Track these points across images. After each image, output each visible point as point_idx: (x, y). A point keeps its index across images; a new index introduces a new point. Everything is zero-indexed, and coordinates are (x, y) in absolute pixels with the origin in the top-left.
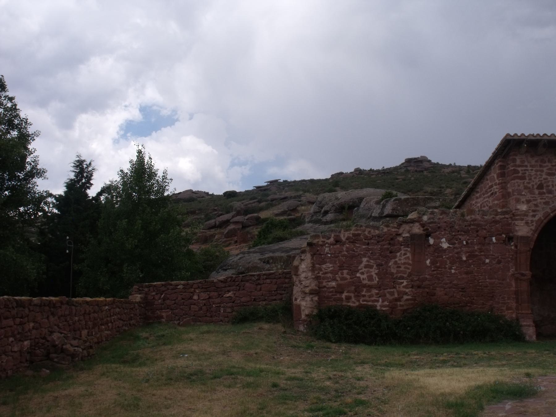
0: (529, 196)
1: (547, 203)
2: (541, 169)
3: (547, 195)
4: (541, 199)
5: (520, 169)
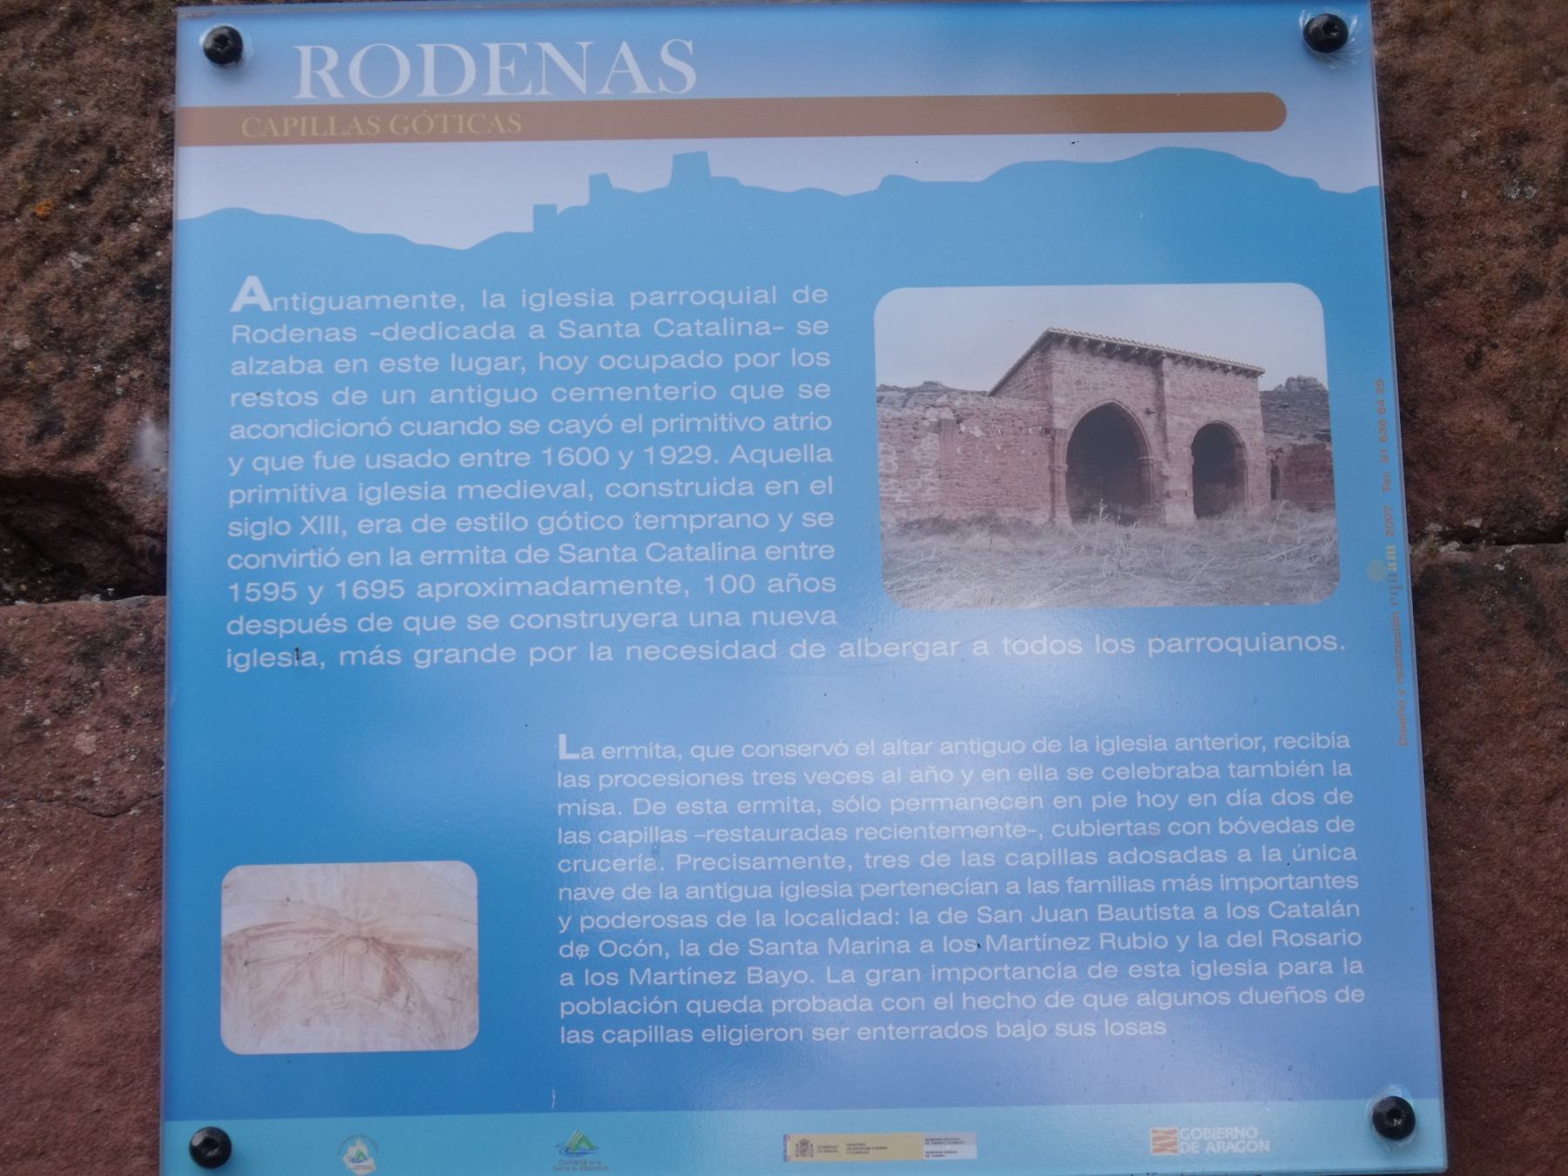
1: (1084, 399)
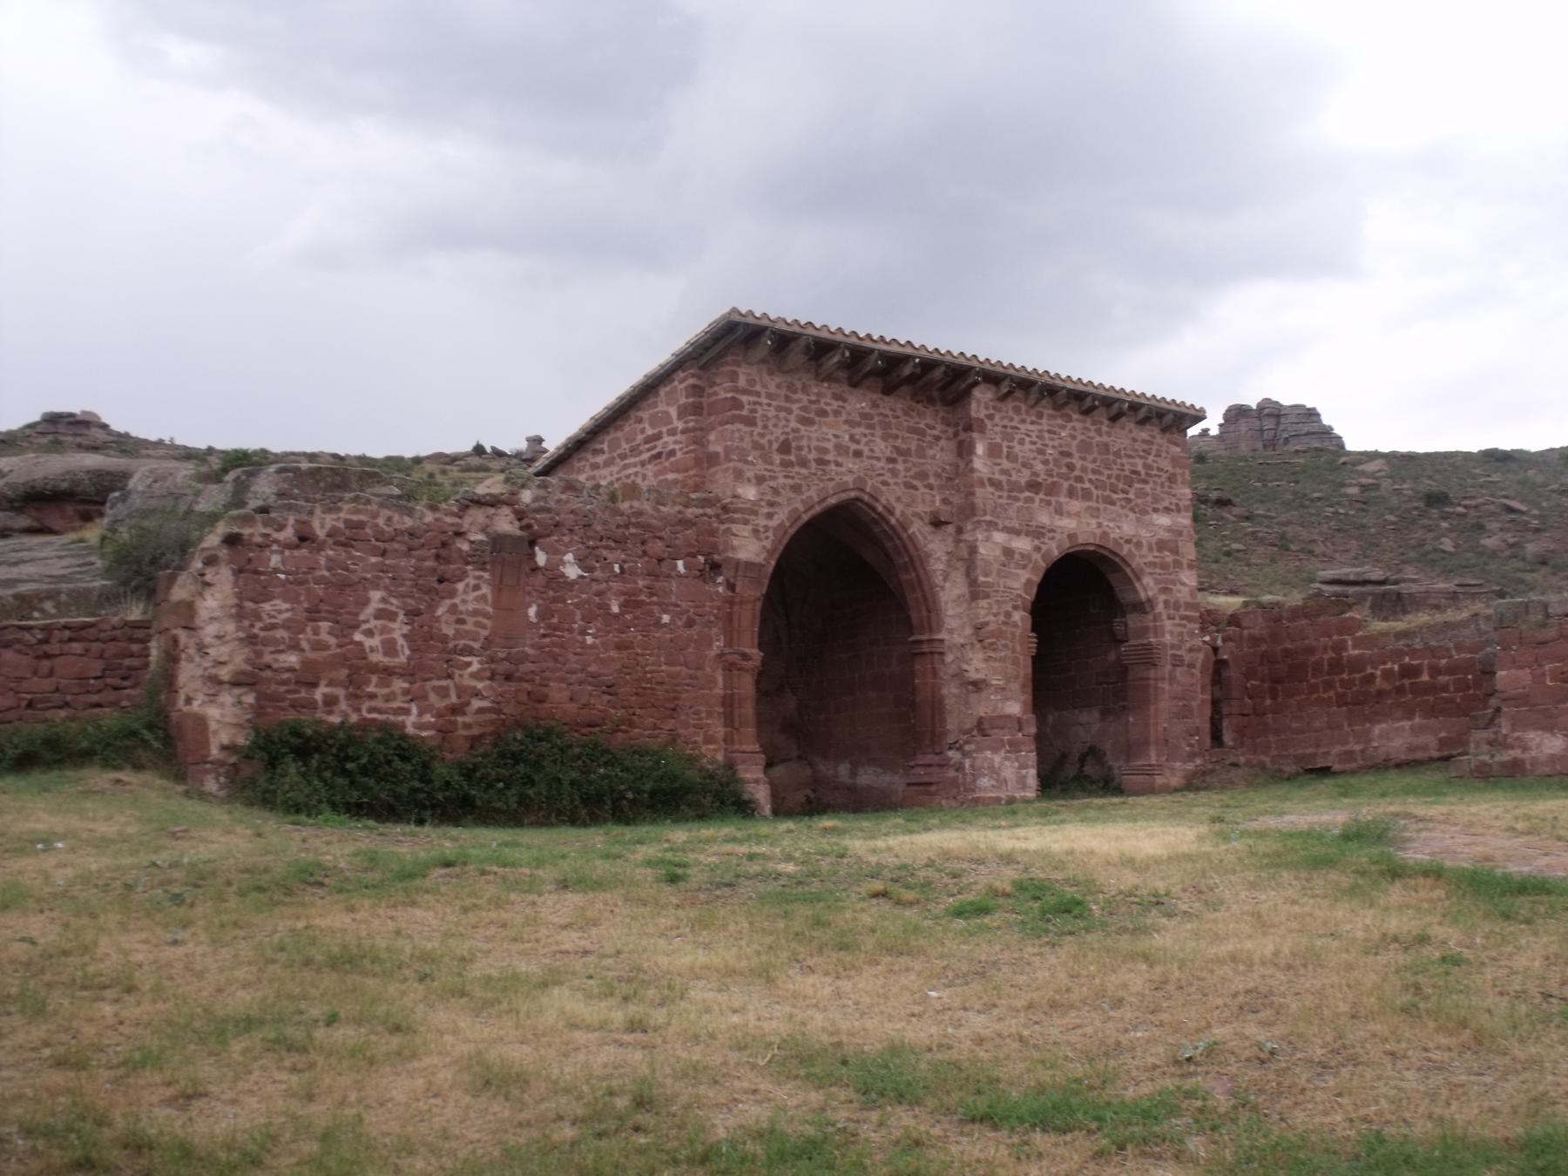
0: (761, 468)
1: (796, 489)
2: (788, 405)
3: (797, 469)
4: (786, 477)
5: (744, 398)
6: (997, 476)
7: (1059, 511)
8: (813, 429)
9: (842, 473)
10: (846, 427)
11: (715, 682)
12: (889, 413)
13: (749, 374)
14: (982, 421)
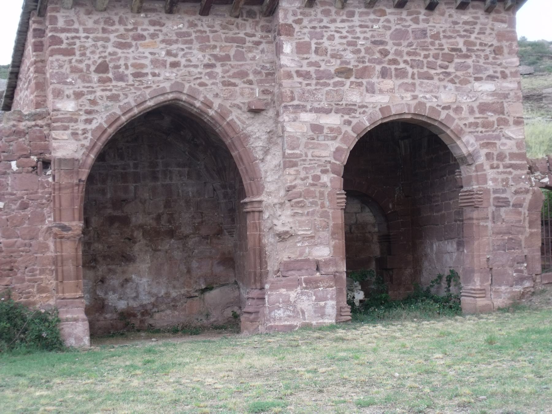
0: (80, 86)
1: (114, 98)
2: (105, 35)
3: (114, 83)
4: (103, 90)
5: (63, 36)
6: (305, 68)
7: (371, 90)
8: (130, 51)
9: (159, 81)
10: (163, 45)
11: (47, 247)
12: (207, 29)
13: (67, 17)
14: (290, 26)
